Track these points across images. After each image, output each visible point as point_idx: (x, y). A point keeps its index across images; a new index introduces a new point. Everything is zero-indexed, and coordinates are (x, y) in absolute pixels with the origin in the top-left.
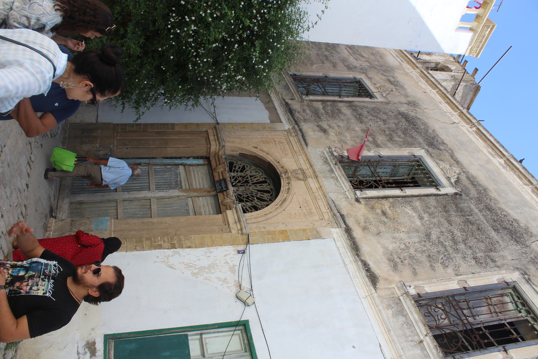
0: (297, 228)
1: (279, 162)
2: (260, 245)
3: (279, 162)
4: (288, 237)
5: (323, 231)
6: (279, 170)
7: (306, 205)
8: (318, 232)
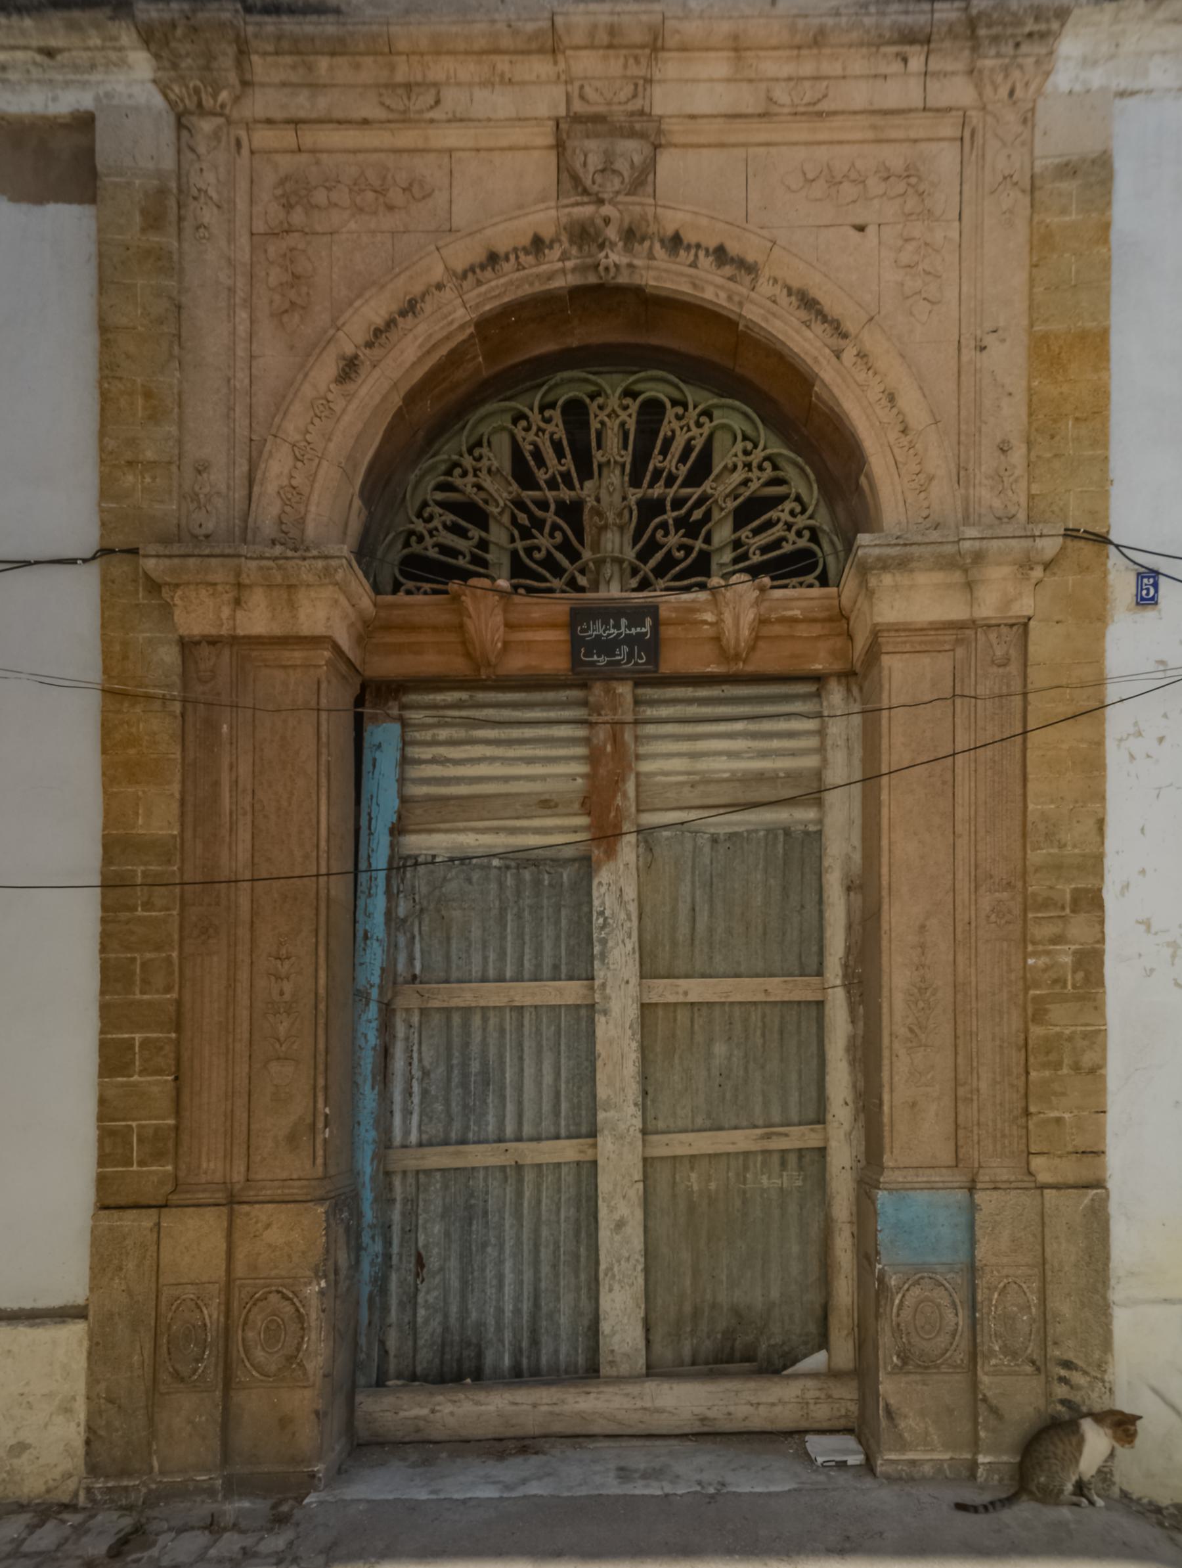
0: (1019, 279)
1: (493, 258)
2: (1117, 493)
3: (493, 258)
4: (1083, 336)
5: (1058, 137)
6: (560, 271)
7: (849, 190)
8: (1068, 170)
